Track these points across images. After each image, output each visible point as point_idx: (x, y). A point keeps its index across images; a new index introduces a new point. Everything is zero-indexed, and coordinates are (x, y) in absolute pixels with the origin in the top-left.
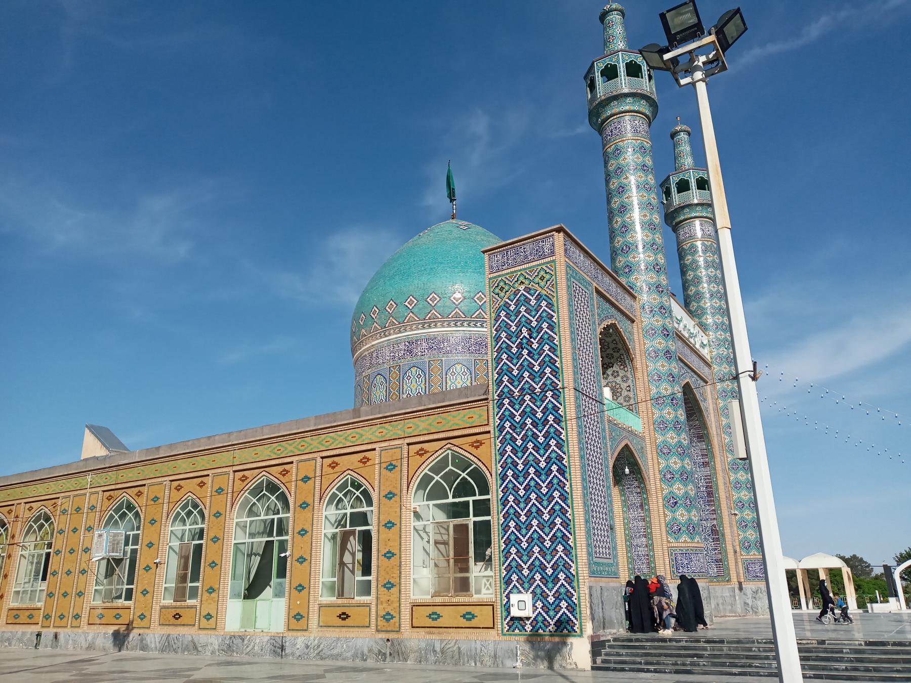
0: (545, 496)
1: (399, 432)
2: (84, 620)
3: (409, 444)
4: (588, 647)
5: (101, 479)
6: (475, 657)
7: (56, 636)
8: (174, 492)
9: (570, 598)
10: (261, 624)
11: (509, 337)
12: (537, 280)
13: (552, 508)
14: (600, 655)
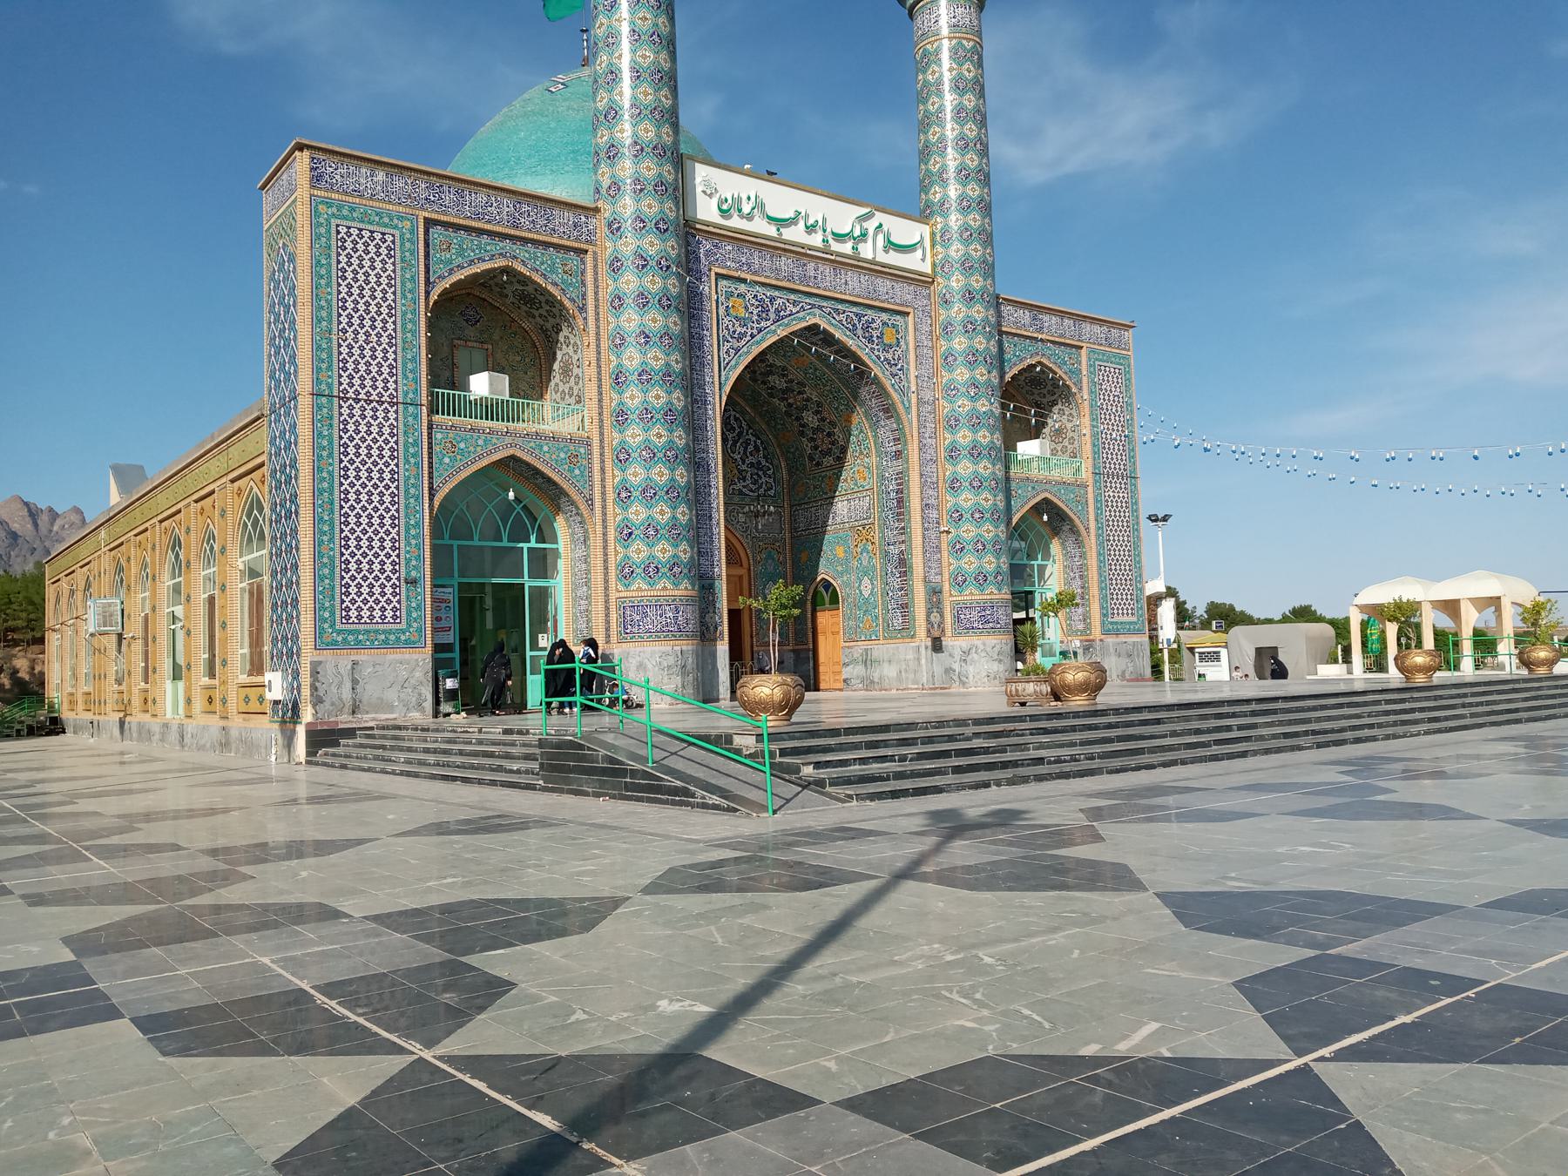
2: (109, 707)
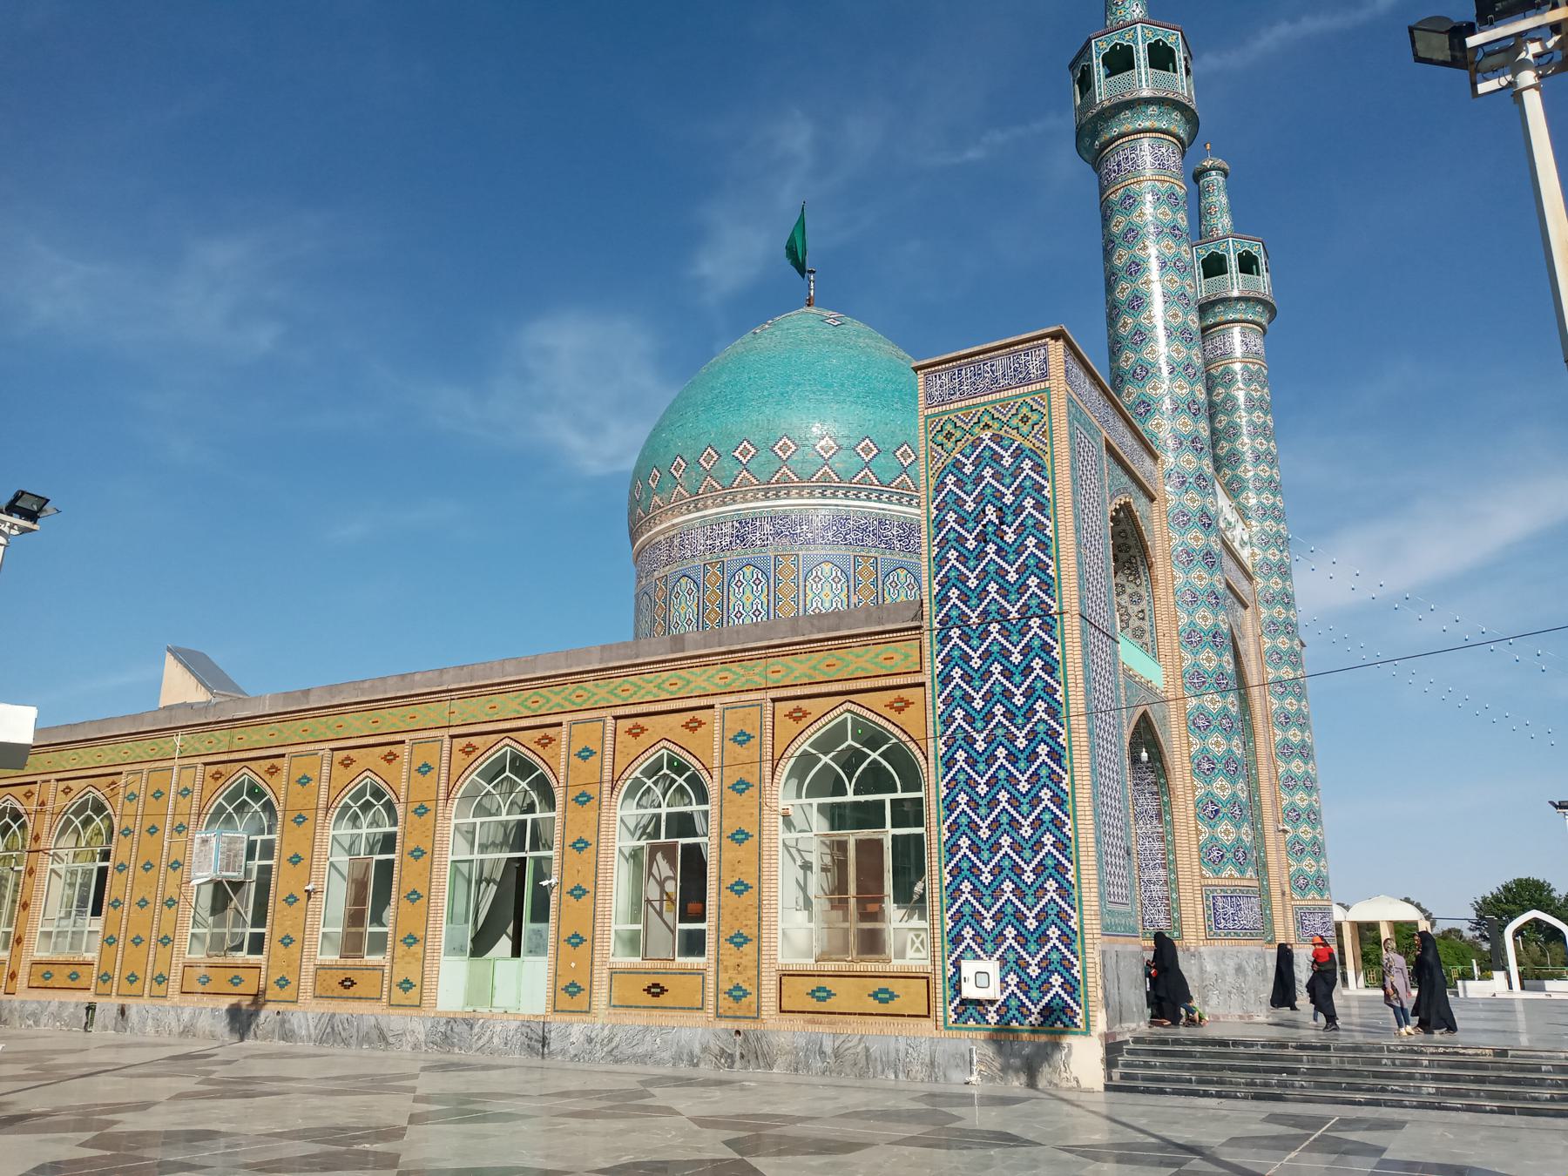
0: (1024, 796)
1: (756, 678)
3: (774, 700)
4: (1100, 1052)
5: (200, 742)
6: (895, 1064)
7: (123, 1011)
8: (338, 770)
9: (1068, 970)
10: (504, 999)
11: (961, 521)
12: (1015, 422)
13: (1037, 818)
14: (1116, 1066)
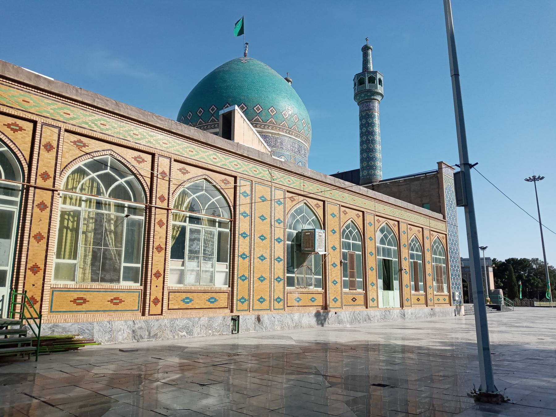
7: (259, 319)
